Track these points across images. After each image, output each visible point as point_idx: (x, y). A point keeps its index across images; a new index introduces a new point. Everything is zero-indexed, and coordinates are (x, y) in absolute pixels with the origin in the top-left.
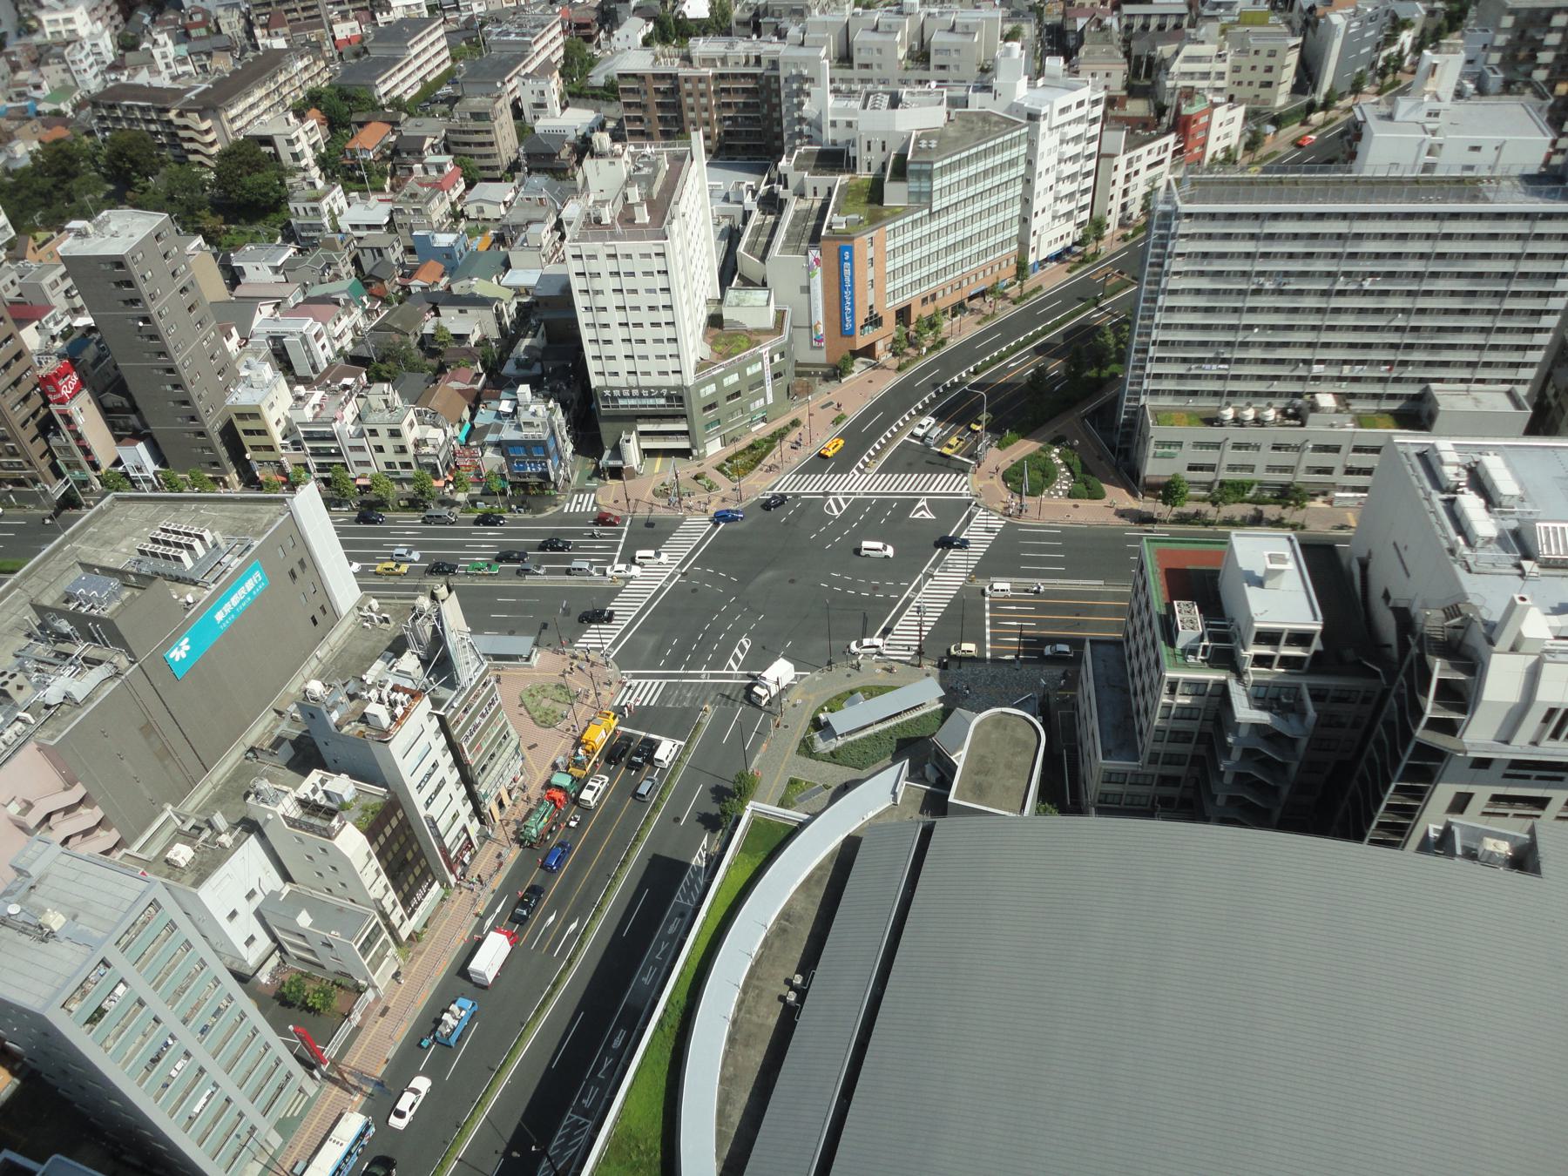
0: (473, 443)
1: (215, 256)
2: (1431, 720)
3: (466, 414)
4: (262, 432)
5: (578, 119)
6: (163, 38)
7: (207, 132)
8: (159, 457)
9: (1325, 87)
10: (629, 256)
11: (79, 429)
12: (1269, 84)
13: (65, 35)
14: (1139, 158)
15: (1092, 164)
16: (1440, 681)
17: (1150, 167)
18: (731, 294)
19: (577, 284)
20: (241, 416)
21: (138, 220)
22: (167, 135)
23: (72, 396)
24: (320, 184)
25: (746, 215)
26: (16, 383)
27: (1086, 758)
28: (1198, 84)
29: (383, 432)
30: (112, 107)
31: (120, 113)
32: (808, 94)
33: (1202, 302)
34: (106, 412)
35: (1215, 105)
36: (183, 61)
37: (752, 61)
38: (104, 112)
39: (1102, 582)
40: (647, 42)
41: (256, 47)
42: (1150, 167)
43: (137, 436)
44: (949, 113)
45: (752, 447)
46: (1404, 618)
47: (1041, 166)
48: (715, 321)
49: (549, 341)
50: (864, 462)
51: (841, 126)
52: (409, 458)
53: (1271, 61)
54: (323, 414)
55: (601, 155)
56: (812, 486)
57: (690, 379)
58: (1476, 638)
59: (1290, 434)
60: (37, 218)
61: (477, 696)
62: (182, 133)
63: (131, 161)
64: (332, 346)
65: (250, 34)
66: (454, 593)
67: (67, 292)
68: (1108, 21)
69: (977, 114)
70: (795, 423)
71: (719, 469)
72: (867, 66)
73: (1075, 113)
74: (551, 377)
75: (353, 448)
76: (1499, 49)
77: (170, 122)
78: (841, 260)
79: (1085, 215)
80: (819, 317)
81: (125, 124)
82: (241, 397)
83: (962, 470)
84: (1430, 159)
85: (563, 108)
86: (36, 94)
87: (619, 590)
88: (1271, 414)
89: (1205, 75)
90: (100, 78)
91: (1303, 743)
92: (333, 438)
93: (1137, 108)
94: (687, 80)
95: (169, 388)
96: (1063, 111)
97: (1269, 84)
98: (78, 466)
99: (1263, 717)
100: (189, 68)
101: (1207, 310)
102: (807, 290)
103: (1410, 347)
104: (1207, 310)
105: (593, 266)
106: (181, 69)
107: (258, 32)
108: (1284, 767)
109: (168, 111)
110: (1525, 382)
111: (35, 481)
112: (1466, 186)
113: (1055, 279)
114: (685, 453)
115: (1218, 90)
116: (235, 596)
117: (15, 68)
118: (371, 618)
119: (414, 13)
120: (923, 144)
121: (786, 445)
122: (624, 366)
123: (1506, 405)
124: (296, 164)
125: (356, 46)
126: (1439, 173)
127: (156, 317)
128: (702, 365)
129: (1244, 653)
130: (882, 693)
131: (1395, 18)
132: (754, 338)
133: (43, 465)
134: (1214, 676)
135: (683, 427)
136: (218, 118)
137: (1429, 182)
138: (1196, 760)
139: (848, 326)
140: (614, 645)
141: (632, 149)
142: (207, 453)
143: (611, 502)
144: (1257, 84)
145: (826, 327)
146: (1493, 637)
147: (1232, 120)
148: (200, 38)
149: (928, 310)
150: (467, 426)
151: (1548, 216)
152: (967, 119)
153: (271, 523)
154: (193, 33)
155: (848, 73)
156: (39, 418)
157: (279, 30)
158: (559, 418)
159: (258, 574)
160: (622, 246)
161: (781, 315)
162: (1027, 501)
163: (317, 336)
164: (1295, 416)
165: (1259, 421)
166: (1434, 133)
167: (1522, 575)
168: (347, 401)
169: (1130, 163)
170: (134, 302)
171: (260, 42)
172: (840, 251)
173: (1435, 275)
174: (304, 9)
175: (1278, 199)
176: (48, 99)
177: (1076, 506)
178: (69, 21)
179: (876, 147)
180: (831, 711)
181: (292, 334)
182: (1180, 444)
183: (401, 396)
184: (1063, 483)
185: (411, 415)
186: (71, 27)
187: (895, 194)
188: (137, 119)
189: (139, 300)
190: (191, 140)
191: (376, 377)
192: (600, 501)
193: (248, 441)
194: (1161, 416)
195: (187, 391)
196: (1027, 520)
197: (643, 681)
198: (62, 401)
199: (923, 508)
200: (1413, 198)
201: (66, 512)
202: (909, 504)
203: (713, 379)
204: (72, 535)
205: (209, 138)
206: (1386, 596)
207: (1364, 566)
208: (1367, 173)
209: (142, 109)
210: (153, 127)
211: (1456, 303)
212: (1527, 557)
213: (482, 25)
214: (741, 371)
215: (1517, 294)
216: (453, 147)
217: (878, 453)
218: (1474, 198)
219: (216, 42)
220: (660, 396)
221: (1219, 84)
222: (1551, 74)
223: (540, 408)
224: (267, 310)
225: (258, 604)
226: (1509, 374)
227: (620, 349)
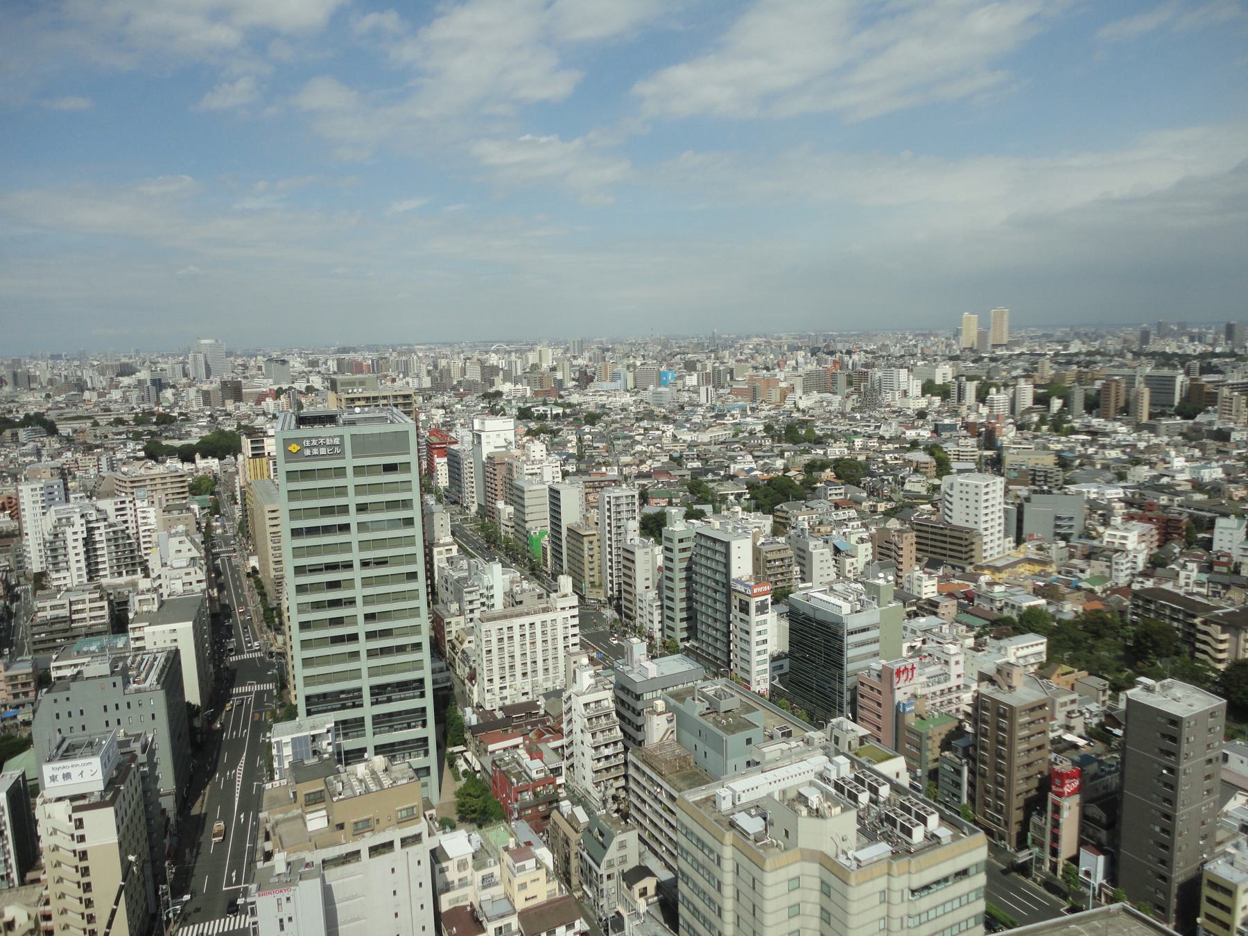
4: (1229, 910)
6: (1192, 566)
7: (1222, 642)
8: (1112, 874)
11: (1061, 820)
13: (1116, 546)
20: (1214, 885)
21: (1198, 696)
22: (1184, 632)
23: (1070, 794)
26: (1029, 765)
30: (1150, 602)
31: (1153, 607)
34: (1085, 818)
36: (1201, 585)
38: (1140, 603)
43: (1099, 849)
60: (1066, 655)
62: (1200, 636)
63: (1154, 642)
67: (1069, 712)
77: (1194, 625)
81: (1152, 615)
82: (1219, 869)
86: (1080, 575)
90: (1128, 578)
95: (1157, 829)
98: (1041, 846)
100: (1204, 591)
106: (1196, 589)
109: (1195, 617)
111: (1002, 838)
117: (1072, 556)
127: (1181, 773)
133: (1015, 829)
136: (1237, 636)
142: (1161, 896)
154: (1216, 568)
156: (1030, 795)
170: (1169, 753)
176: (1086, 580)
178: (1124, 538)
186: (1123, 541)
188: (1165, 615)
189: (1173, 754)
190: (1205, 643)
193: (1206, 907)
195: (1173, 839)
198: (1060, 795)
201: (1015, 874)
204: (1080, 919)
205: (1222, 647)
209: (1173, 609)
210: (1175, 624)
219: (1235, 578)
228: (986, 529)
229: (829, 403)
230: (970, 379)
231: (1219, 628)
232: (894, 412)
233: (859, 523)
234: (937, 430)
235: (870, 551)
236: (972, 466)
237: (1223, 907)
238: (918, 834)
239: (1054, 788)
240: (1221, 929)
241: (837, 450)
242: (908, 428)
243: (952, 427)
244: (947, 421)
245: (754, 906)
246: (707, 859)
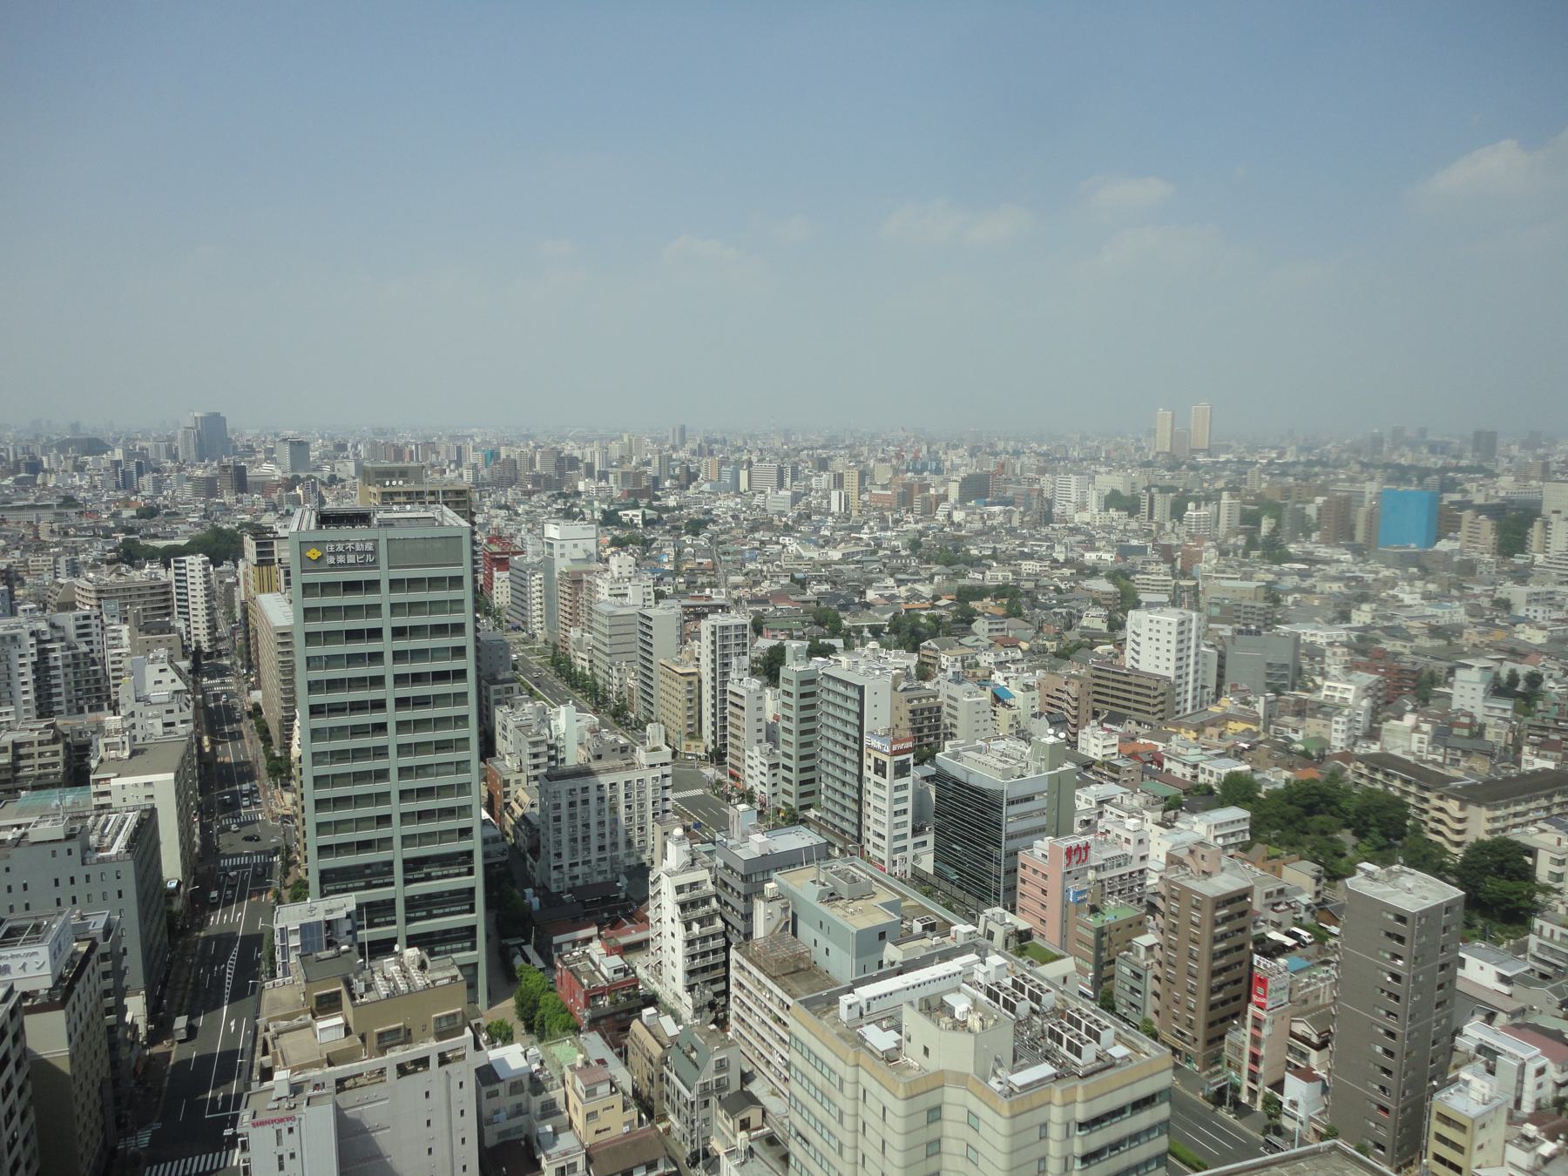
20: (1446, 1120)
41: (1518, 763)
95: (1379, 1049)
98: (1239, 1069)
107: (1526, 749)
157: (1549, 754)
171: (1524, 757)
219: (1475, 743)
228: (1180, 677)
229: (991, 516)
230: (1164, 490)
231: (1457, 803)
232: (1071, 529)
233: (1025, 666)
234: (1124, 551)
235: (1038, 701)
236: (1165, 598)
238: (1090, 1051)
239: (1255, 998)
241: (997, 575)
242: (1088, 549)
243: (1141, 550)
244: (1134, 542)
245: (883, 1142)
246: (826, 1081)
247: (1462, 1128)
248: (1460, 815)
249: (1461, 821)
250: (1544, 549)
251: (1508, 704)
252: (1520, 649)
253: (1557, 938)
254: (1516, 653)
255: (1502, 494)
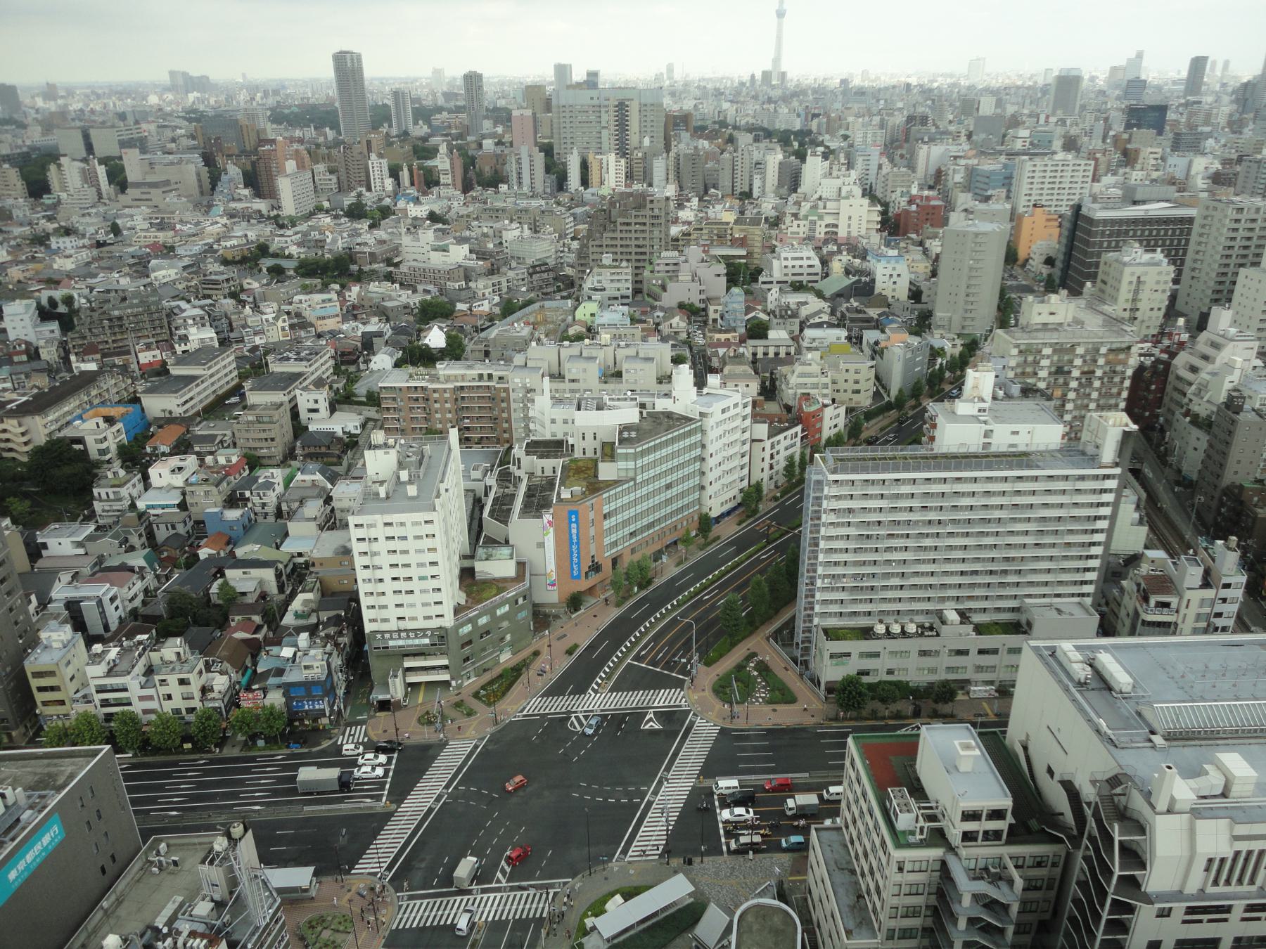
0: (255, 687)
1: (22, 534)
2: (1120, 877)
3: (248, 663)
5: (346, 422)
9: (894, 392)
10: (402, 524)
12: (858, 392)
14: (779, 442)
15: (747, 447)
16: (1120, 842)
17: (786, 449)
18: (481, 552)
19: (357, 548)
24: (122, 473)
25: (487, 490)
27: (827, 940)
28: (812, 392)
29: (173, 679)
32: (533, 401)
33: (852, 546)
35: (826, 406)
37: (486, 377)
39: (807, 775)
40: (397, 365)
41: (70, 370)
42: (786, 449)
44: (641, 413)
45: (501, 676)
46: (1070, 788)
47: (711, 448)
48: (467, 575)
49: (323, 595)
50: (597, 684)
51: (559, 421)
52: (196, 703)
53: (857, 377)
54: (116, 669)
55: (376, 447)
56: (557, 706)
57: (448, 621)
58: (1137, 803)
59: (927, 643)
61: (269, 934)
64: (124, 607)
65: (66, 361)
66: (250, 833)
68: (741, 350)
69: (663, 413)
70: (536, 654)
71: (476, 695)
72: (573, 381)
73: (732, 412)
74: (326, 625)
75: (142, 698)
76: (1012, 369)
78: (570, 522)
79: (745, 483)
80: (551, 566)
83: (679, 684)
84: (987, 440)
85: (333, 409)
87: (391, 814)
88: (912, 628)
89: (815, 386)
91: (1015, 908)
92: (125, 690)
93: (772, 408)
94: (435, 391)
96: (723, 411)
97: (858, 392)
99: (983, 887)
101: (856, 550)
102: (541, 545)
103: (1005, 572)
104: (856, 550)
105: (373, 533)
107: (73, 358)
108: (1001, 931)
110: (1088, 595)
112: (1020, 458)
113: (729, 530)
114: (446, 684)
115: (825, 396)
116: (31, 853)
118: (160, 862)
119: (208, 342)
120: (626, 435)
121: (532, 672)
122: (392, 613)
123: (1079, 613)
124: (103, 458)
125: (157, 367)
126: (993, 449)
128: (458, 610)
129: (954, 831)
130: (637, 894)
131: (932, 348)
132: (501, 585)
134: (937, 853)
135: (445, 662)
137: (987, 456)
138: (927, 931)
139: (575, 573)
140: (389, 868)
141: (403, 442)
143: (380, 732)
144: (850, 391)
145: (558, 575)
146: (1152, 800)
147: (838, 416)
148: (21, 363)
149: (637, 557)
150: (249, 672)
151: (1082, 478)
152: (655, 417)
153: (72, 777)
155: (561, 386)
157: (90, 357)
158: (337, 661)
159: (56, 828)
160: (395, 518)
161: (521, 565)
162: (736, 708)
163: (112, 600)
164: (931, 628)
165: (904, 634)
166: (985, 422)
167: (1154, 747)
168: (140, 656)
169: (772, 447)
172: (571, 513)
173: (1014, 520)
174: (114, 341)
175: (896, 470)
177: (774, 710)
179: (589, 437)
180: (596, 916)
181: (89, 598)
182: (848, 655)
183: (191, 648)
184: (762, 694)
185: (201, 665)
187: (606, 471)
191: (165, 633)
192: (371, 733)
193: (40, 697)
194: (831, 634)
196: (739, 724)
197: (418, 902)
199: (651, 720)
200: (989, 467)
202: (639, 716)
203: (470, 621)
206: (1050, 771)
207: (1025, 748)
208: (944, 450)
211: (1030, 540)
212: (1153, 733)
213: (266, 353)
214: (491, 611)
215: (1071, 532)
216: (240, 442)
217: (609, 677)
218: (1029, 467)
219: (35, 364)
220: (425, 636)
221: (825, 391)
222: (1048, 384)
223: (316, 653)
224: (66, 577)
225: (52, 859)
226: (1076, 590)
227: (390, 599)
237: (52, 689)
240: (59, 708)
247: (52, 674)
248: (22, 430)
249: (23, 434)
250: (64, 188)
251: (55, 326)
252: (56, 277)
253: (112, 496)
254: (53, 282)
255: (28, 143)
